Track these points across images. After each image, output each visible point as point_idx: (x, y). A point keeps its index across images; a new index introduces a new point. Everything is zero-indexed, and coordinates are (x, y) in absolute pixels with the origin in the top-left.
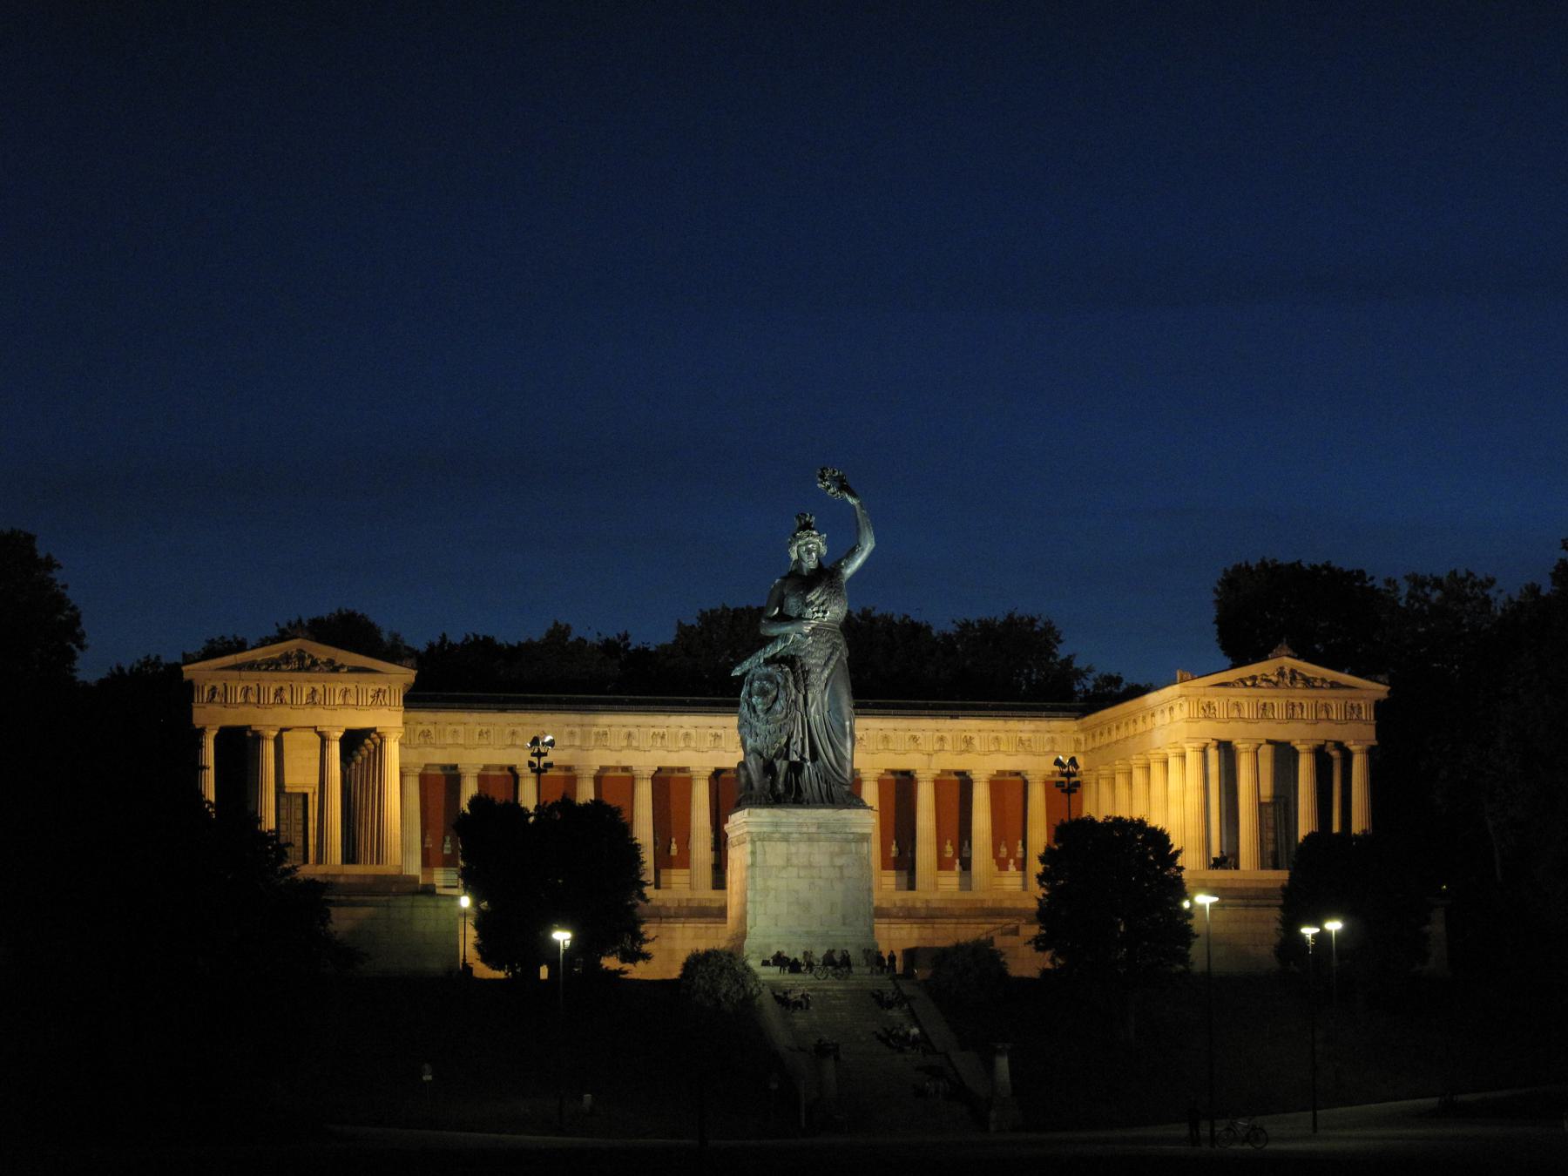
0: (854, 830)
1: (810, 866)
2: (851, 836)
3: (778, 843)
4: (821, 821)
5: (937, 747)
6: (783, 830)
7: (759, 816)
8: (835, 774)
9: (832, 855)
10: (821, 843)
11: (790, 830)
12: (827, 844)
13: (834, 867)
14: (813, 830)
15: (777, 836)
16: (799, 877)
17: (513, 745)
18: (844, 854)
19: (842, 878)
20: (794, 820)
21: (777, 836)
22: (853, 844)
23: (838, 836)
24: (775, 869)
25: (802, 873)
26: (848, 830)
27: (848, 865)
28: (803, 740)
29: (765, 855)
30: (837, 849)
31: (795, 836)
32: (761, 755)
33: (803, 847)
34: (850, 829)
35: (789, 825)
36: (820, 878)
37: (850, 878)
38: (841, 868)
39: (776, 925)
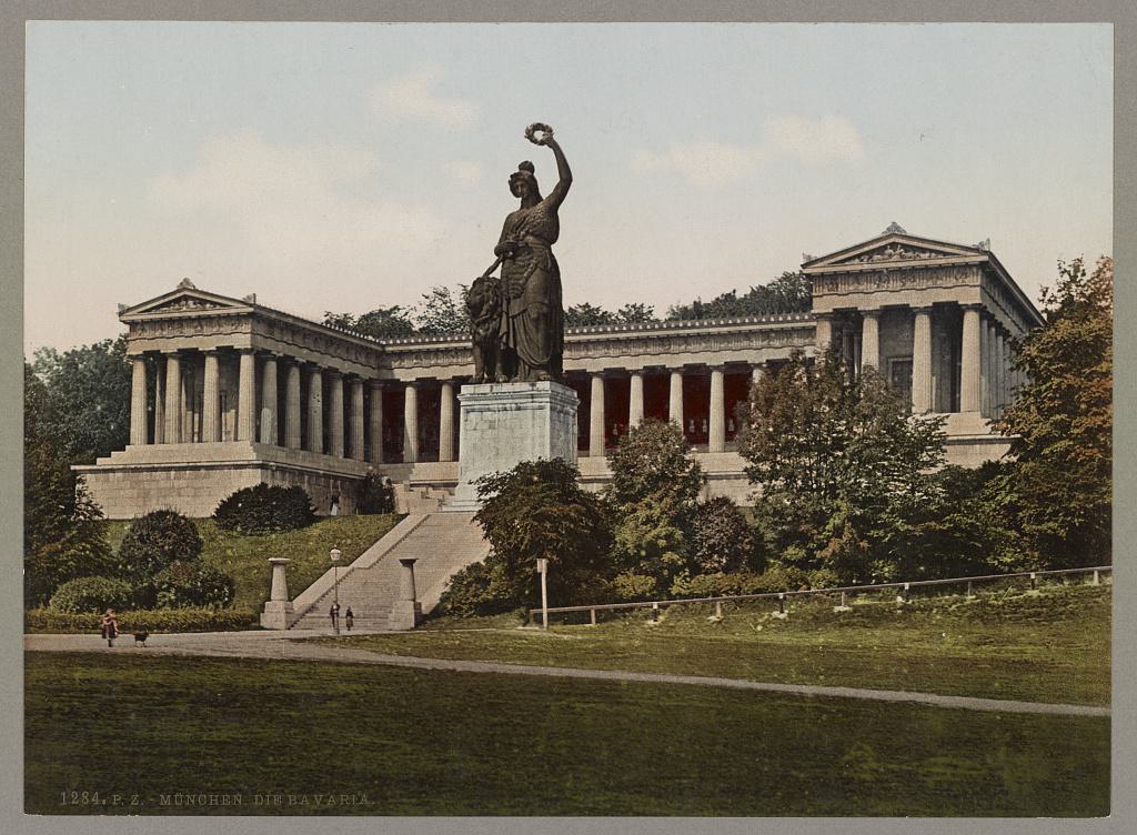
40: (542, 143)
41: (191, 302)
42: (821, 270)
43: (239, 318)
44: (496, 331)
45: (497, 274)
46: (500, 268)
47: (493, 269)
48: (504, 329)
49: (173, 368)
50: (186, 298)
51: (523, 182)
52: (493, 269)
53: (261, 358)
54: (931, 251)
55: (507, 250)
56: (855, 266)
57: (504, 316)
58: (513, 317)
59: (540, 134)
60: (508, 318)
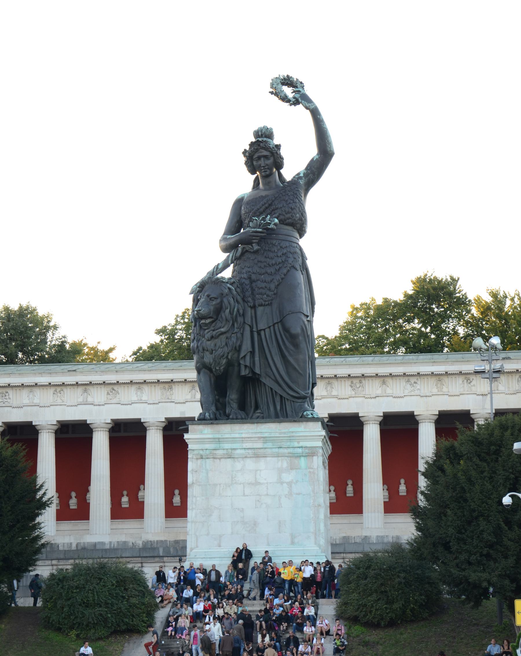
0: (302, 444)
1: (257, 483)
2: (300, 450)
3: (222, 460)
4: (266, 435)
6: (227, 446)
7: (201, 433)
8: (287, 390)
9: (280, 471)
10: (268, 459)
11: (235, 446)
12: (275, 459)
13: (282, 483)
14: (259, 445)
15: (220, 452)
16: (244, 495)
18: (292, 469)
19: (290, 495)
20: (237, 436)
21: (220, 452)
22: (302, 458)
23: (286, 451)
24: (219, 485)
25: (248, 491)
26: (296, 444)
27: (297, 481)
28: (252, 353)
29: (207, 474)
30: (285, 465)
31: (238, 451)
32: (210, 370)
33: (250, 464)
34: (298, 442)
35: (234, 440)
36: (267, 495)
37: (299, 494)
38: (290, 484)
39: (220, 546)
44: (238, 350)
47: (226, 266)
48: (246, 346)
52: (226, 266)
57: (247, 328)
58: (264, 330)
60: (252, 332)
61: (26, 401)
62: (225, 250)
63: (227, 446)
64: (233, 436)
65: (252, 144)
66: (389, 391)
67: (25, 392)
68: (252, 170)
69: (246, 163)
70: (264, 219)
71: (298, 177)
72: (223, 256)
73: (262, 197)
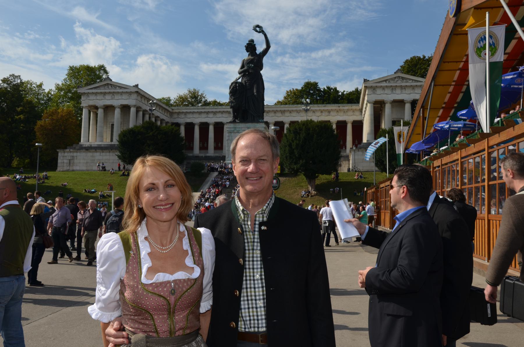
3: (236, 133)
5: (320, 114)
6: (237, 129)
15: (235, 131)
17: (207, 117)
35: (239, 128)
40: (259, 32)
41: (110, 87)
42: (371, 85)
43: (130, 93)
45: (240, 80)
46: (241, 78)
47: (239, 78)
49: (100, 112)
50: (108, 84)
51: (251, 47)
52: (239, 78)
53: (138, 109)
54: (413, 80)
55: (243, 72)
56: (384, 84)
59: (258, 29)
61: (191, 116)
62: (240, 74)
63: (237, 129)
64: (239, 126)
65: (247, 44)
66: (292, 115)
67: (191, 114)
68: (248, 51)
69: (246, 49)
70: (250, 65)
71: (260, 53)
72: (238, 76)
73: (250, 59)
